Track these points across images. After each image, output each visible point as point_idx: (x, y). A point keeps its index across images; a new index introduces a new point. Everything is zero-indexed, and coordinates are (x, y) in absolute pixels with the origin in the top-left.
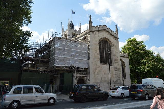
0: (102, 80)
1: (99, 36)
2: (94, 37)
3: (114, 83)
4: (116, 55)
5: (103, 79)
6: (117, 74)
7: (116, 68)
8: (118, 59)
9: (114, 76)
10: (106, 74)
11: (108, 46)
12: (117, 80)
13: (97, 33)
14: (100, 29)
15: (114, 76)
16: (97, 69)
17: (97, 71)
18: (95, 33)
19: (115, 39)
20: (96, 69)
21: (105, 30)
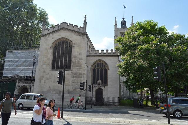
1: (53, 38)
2: (45, 41)
3: (69, 93)
5: (52, 88)
6: (76, 81)
7: (76, 73)
8: (81, 61)
9: (71, 84)
11: (66, 47)
13: (51, 35)
14: (54, 30)
15: (71, 84)
16: (45, 77)
17: (44, 79)
18: (47, 36)
20: (43, 77)
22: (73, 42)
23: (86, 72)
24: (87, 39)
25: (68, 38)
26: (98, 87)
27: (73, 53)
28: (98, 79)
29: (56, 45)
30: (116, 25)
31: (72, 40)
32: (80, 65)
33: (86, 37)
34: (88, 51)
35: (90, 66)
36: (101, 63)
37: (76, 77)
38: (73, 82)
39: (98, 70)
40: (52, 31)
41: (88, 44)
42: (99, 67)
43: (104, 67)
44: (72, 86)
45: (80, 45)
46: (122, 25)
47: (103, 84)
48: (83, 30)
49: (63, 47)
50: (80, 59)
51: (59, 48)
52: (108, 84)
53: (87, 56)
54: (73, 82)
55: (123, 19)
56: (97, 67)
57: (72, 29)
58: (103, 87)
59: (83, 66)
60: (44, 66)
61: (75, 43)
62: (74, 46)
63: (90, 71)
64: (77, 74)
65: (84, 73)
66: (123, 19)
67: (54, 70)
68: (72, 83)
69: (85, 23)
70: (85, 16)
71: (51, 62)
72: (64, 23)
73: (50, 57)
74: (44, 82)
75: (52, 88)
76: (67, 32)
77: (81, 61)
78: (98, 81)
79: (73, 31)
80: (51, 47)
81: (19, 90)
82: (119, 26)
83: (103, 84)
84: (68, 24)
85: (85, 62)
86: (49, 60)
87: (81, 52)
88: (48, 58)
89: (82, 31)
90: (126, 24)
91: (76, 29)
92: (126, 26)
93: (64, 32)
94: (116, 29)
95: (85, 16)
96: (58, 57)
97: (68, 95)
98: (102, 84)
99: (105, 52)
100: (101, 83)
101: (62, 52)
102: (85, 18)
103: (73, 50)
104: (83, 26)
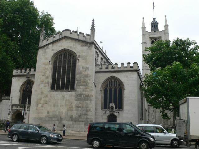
0: (49, 116)
1: (53, 50)
2: (43, 54)
3: (72, 121)
4: (83, 73)
5: (51, 114)
6: (81, 105)
7: (80, 95)
10: (57, 106)
11: (69, 61)
12: (80, 116)
13: (51, 46)
14: (55, 39)
15: (74, 108)
16: (43, 99)
17: (42, 102)
18: (46, 47)
19: (86, 46)
20: (41, 99)
21: (65, 37)
22: (78, 54)
23: (93, 93)
24: (96, 50)
25: (71, 49)
26: (110, 113)
27: (77, 68)
28: (111, 102)
29: (57, 58)
30: (144, 28)
31: (75, 52)
32: (86, 85)
33: (93, 47)
34: (97, 65)
35: (99, 86)
36: (114, 81)
37: (81, 99)
38: (77, 107)
39: (111, 90)
40: (52, 41)
41: (98, 56)
42: (112, 86)
43: (119, 86)
44: (76, 112)
45: (86, 58)
46: (152, 27)
47: (118, 108)
48: (90, 39)
49: (65, 61)
50: (86, 76)
51: (60, 62)
52: (123, 109)
53: (96, 72)
54: (77, 107)
55: (154, 19)
56: (110, 86)
57: (76, 37)
58: (116, 112)
59: (89, 85)
60: (42, 85)
61: (79, 56)
62: (78, 60)
63: (100, 92)
64: (82, 95)
65: (91, 94)
66: (154, 19)
67: (54, 91)
68: (76, 108)
69: (93, 29)
70: (93, 20)
71: (50, 80)
72: (66, 30)
73: (50, 74)
74: (42, 107)
75: (51, 114)
76: (69, 41)
77: (87, 79)
78: (111, 105)
79: (77, 40)
80: (50, 62)
81: (13, 115)
82: (149, 29)
83: (118, 108)
84: (72, 32)
85: (93, 80)
86: (47, 77)
87: (87, 66)
88: (47, 75)
89: (88, 40)
90: (157, 26)
91: (81, 38)
92: (158, 29)
93: (66, 41)
94: (144, 33)
95: (93, 20)
96: (59, 74)
97: (71, 123)
98: (116, 108)
99: (119, 65)
100: (114, 107)
101: (64, 68)
102: (93, 23)
103: (77, 64)
104: (90, 34)
